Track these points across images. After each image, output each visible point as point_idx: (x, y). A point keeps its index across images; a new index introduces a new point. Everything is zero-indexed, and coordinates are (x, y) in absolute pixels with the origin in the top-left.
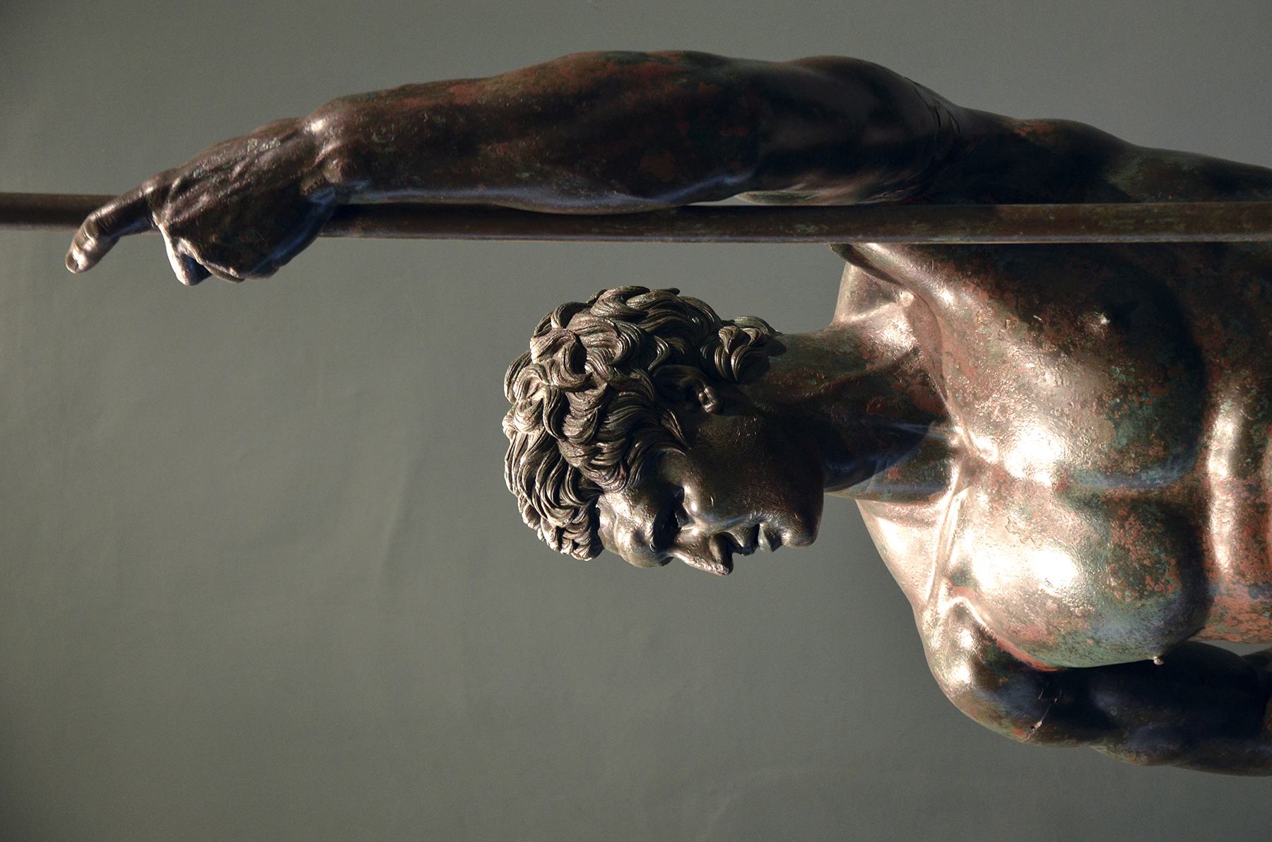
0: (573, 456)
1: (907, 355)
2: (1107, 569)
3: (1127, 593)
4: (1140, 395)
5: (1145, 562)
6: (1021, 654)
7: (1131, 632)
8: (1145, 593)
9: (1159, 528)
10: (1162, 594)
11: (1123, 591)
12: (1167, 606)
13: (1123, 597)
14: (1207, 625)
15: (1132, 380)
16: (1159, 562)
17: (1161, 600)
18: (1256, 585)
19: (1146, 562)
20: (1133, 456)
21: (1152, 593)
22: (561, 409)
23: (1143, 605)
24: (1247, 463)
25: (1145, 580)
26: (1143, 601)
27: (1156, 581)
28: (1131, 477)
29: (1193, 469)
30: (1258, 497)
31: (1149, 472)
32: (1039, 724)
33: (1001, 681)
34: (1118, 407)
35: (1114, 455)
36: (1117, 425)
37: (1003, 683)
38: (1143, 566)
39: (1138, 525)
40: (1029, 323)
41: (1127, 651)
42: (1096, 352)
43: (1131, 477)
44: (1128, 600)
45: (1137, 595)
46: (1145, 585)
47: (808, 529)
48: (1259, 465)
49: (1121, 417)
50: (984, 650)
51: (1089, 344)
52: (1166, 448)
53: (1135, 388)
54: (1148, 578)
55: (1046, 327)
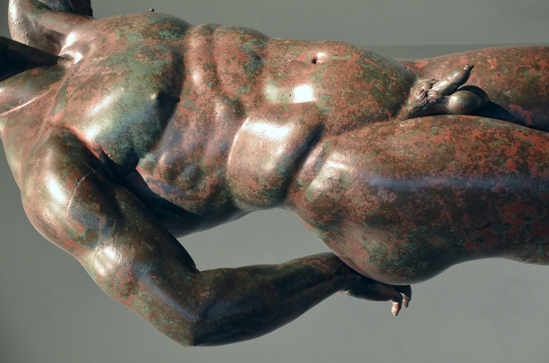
2: (138, 52)
5: (157, 49)
7: (145, 76)
8: (155, 58)
10: (162, 60)
11: (144, 58)
12: (165, 66)
14: (181, 97)
16: (164, 50)
18: (207, 64)
21: (158, 59)
23: (153, 63)
24: (208, 32)
25: (155, 54)
26: (153, 61)
28: (154, 33)
29: (183, 39)
30: (211, 44)
31: (163, 32)
32: (84, 178)
33: (68, 144)
37: (69, 145)
41: (141, 91)
43: (154, 33)
45: (151, 59)
48: (212, 33)
52: (172, 25)
54: (157, 54)
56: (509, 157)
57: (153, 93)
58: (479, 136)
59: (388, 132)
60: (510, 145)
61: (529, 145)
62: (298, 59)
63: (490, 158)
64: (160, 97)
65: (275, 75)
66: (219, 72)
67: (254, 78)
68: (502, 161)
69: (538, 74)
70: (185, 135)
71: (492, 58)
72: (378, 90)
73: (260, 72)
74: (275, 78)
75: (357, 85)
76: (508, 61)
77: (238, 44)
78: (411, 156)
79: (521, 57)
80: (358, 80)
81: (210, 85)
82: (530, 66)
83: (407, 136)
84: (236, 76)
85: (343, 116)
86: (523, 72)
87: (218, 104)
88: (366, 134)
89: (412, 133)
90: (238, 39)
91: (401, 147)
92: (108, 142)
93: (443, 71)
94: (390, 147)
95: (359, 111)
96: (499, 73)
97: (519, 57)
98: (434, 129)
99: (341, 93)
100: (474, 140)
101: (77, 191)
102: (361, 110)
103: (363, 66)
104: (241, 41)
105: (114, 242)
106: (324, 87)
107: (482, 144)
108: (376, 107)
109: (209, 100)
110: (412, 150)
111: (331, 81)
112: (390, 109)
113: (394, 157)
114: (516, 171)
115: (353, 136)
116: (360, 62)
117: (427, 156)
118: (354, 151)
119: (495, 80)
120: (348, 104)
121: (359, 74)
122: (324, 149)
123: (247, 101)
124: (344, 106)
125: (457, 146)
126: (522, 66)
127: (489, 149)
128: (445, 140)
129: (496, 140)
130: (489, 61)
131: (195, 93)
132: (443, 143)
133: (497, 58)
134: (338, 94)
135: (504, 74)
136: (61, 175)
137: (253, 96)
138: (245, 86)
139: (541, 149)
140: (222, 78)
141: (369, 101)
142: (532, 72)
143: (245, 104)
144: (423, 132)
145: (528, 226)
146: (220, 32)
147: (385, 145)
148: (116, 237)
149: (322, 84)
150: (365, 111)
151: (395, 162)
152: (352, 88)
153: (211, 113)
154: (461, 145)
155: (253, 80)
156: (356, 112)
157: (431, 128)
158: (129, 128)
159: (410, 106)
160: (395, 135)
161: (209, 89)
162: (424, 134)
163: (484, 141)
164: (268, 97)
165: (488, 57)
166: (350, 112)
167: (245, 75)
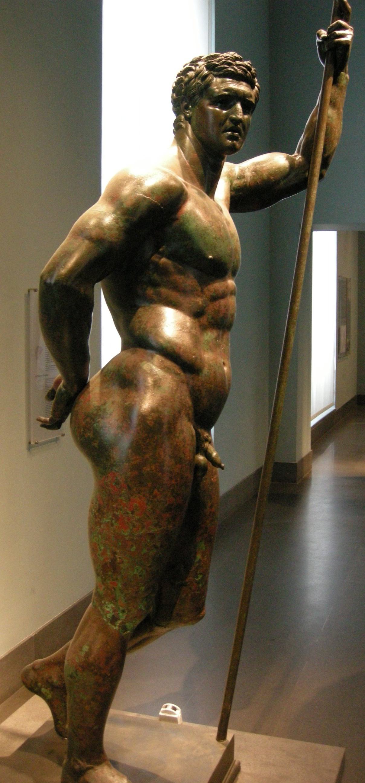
70: (182, 277)
78: (178, 435)
81: (214, 295)
85: (199, 387)
92: (182, 224)
99: (212, 384)
101: (155, 202)
105: (120, 227)
110: (181, 435)
113: (177, 423)
122: (179, 374)
123: (204, 320)
138: (213, 318)
140: (217, 302)
145: (128, 513)
148: (123, 229)
151: (174, 424)
153: (197, 295)
158: (190, 239)
161: (211, 294)
164: (205, 334)
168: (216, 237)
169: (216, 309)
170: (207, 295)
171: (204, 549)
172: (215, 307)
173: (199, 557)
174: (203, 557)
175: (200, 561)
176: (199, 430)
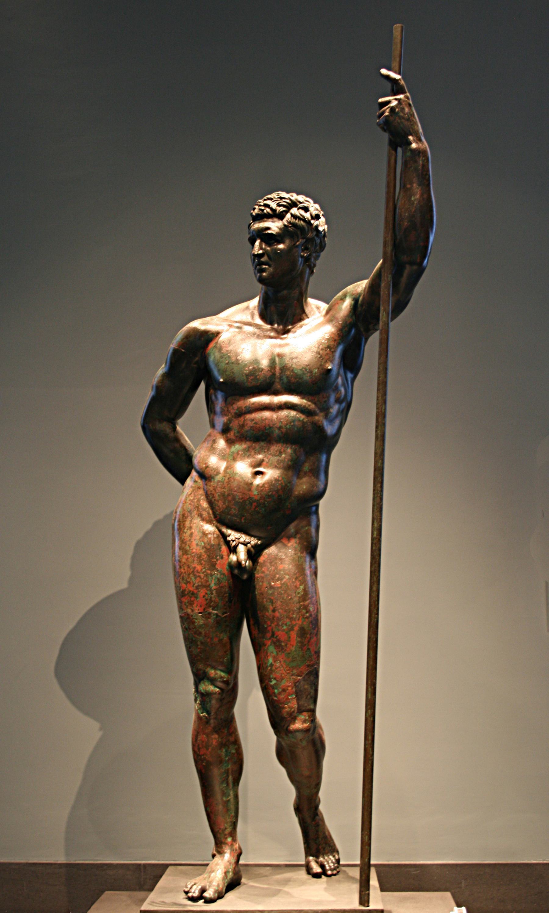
0: (294, 211)
1: (306, 315)
2: (255, 366)
3: (247, 372)
4: (310, 376)
6: (212, 345)
9: (268, 381)
11: (248, 370)
13: (246, 370)
15: (314, 374)
17: (245, 381)
19: (258, 377)
20: (291, 374)
21: (248, 378)
22: (306, 209)
23: (243, 376)
25: (253, 376)
27: (252, 380)
34: (306, 370)
35: (291, 369)
36: (301, 370)
38: (257, 376)
39: (269, 375)
40: (327, 348)
42: (321, 365)
44: (245, 372)
46: (250, 376)
47: (261, 280)
49: (303, 371)
50: (213, 334)
51: (323, 363)
53: (312, 375)
55: (326, 352)
56: (186, 585)
57: (223, 379)
58: (196, 569)
59: (203, 517)
60: (193, 586)
61: (197, 598)
62: (264, 463)
63: (185, 575)
64: (222, 382)
65: (247, 449)
66: (245, 415)
67: (243, 437)
68: (185, 582)
69: (270, 611)
71: (281, 584)
72: (230, 511)
73: (250, 440)
74: (244, 450)
75: (230, 498)
76: (277, 593)
77: (276, 425)
78: (185, 531)
79: (281, 602)
80: (234, 499)
81: (237, 412)
82: (274, 606)
83: (198, 528)
84: (243, 426)
85: (211, 491)
86: (270, 602)
87: (227, 418)
88: (202, 505)
89: (200, 531)
90: (280, 424)
91: (191, 525)
93: (274, 554)
94: (193, 519)
95: (215, 500)
96: (268, 587)
97: (281, 600)
98: (201, 544)
100: (193, 566)
102: (216, 501)
103: (248, 502)
104: (278, 427)
106: (228, 479)
107: (192, 570)
108: (219, 510)
109: (230, 412)
110: (188, 531)
111: (232, 482)
112: (220, 518)
113: (186, 521)
114: (181, 589)
115: (202, 497)
116: (251, 499)
117: (185, 540)
118: (192, 498)
119: (263, 585)
120: (218, 494)
121: (239, 499)
123: (231, 435)
124: (217, 491)
125: (189, 556)
126: (274, 602)
127: (189, 574)
128: (192, 549)
129: (195, 578)
130: (278, 582)
131: (234, 403)
132: (191, 548)
133: (281, 587)
134: (225, 487)
135: (268, 590)
136: (184, 339)
137: (233, 438)
138: (238, 432)
139: (195, 604)
141: (222, 506)
142: (271, 608)
143: (229, 434)
144: (199, 538)
146: (290, 413)
147: (194, 516)
149: (230, 478)
150: (216, 504)
151: (183, 521)
152: (229, 495)
153: (224, 415)
154: (190, 558)
155: (242, 436)
156: (214, 498)
157: (203, 542)
159: (224, 530)
160: (200, 522)
161: (235, 411)
162: (198, 538)
163: (193, 572)
164: (233, 447)
165: (282, 582)
166: (213, 494)
167: (244, 431)
168: (228, 362)
169: (241, 424)
170: (232, 413)
171: (275, 653)
172: (240, 422)
173: (271, 660)
174: (275, 661)
175: (271, 665)
176: (224, 530)
